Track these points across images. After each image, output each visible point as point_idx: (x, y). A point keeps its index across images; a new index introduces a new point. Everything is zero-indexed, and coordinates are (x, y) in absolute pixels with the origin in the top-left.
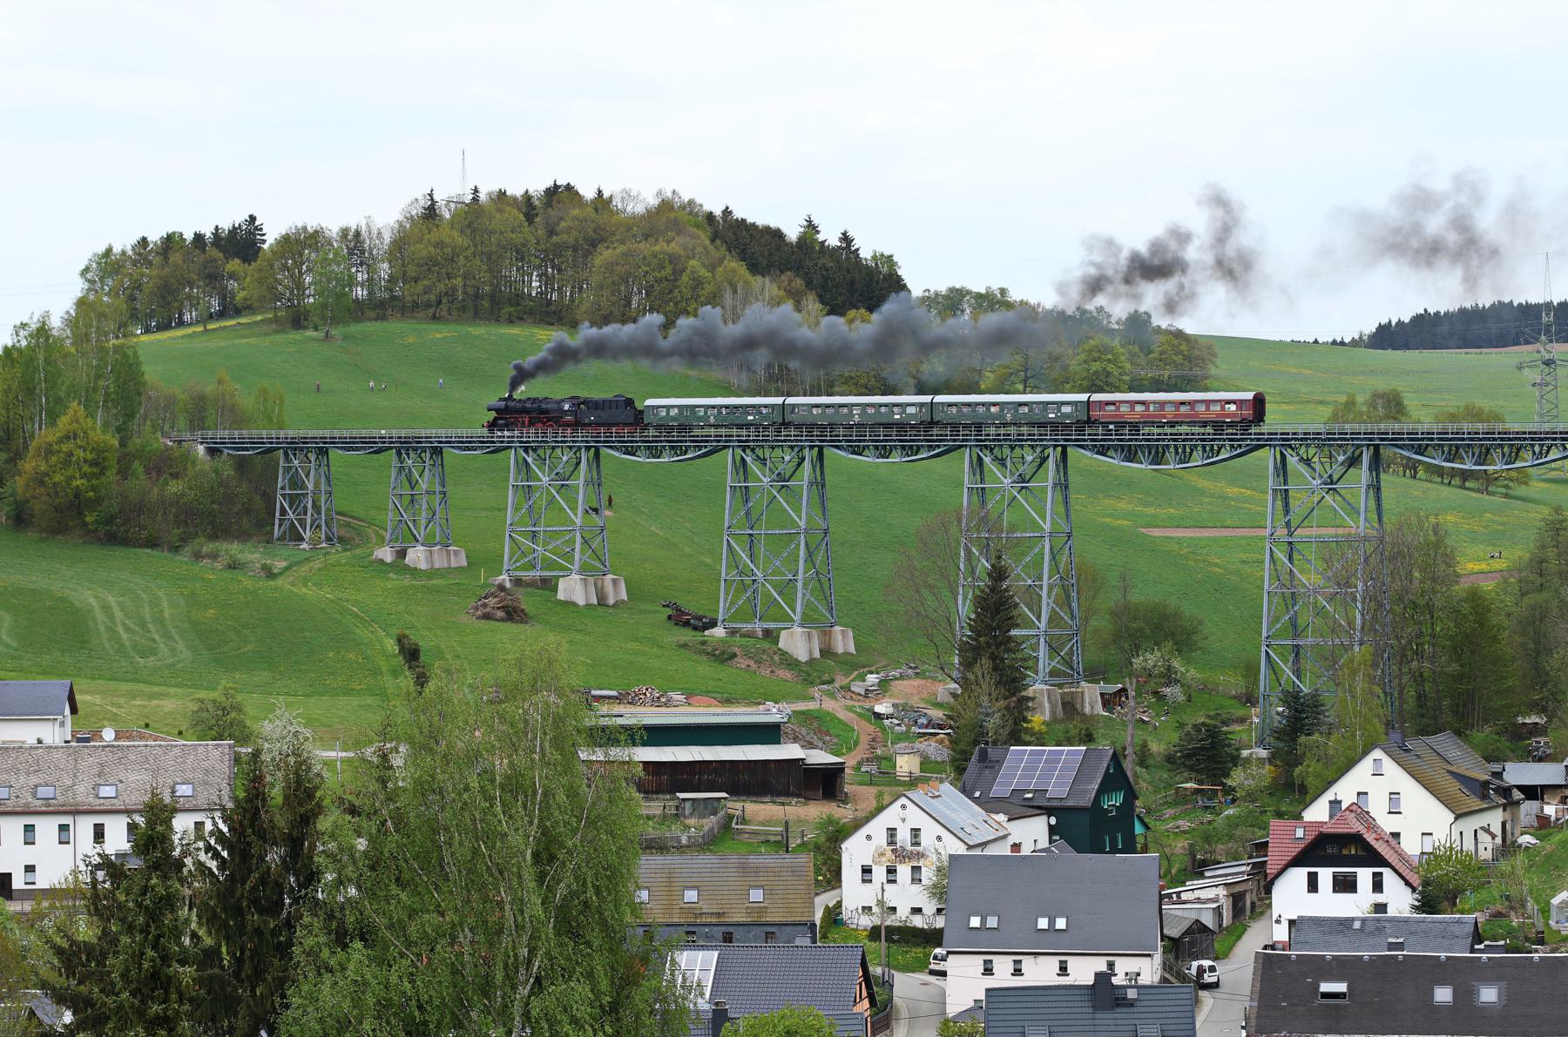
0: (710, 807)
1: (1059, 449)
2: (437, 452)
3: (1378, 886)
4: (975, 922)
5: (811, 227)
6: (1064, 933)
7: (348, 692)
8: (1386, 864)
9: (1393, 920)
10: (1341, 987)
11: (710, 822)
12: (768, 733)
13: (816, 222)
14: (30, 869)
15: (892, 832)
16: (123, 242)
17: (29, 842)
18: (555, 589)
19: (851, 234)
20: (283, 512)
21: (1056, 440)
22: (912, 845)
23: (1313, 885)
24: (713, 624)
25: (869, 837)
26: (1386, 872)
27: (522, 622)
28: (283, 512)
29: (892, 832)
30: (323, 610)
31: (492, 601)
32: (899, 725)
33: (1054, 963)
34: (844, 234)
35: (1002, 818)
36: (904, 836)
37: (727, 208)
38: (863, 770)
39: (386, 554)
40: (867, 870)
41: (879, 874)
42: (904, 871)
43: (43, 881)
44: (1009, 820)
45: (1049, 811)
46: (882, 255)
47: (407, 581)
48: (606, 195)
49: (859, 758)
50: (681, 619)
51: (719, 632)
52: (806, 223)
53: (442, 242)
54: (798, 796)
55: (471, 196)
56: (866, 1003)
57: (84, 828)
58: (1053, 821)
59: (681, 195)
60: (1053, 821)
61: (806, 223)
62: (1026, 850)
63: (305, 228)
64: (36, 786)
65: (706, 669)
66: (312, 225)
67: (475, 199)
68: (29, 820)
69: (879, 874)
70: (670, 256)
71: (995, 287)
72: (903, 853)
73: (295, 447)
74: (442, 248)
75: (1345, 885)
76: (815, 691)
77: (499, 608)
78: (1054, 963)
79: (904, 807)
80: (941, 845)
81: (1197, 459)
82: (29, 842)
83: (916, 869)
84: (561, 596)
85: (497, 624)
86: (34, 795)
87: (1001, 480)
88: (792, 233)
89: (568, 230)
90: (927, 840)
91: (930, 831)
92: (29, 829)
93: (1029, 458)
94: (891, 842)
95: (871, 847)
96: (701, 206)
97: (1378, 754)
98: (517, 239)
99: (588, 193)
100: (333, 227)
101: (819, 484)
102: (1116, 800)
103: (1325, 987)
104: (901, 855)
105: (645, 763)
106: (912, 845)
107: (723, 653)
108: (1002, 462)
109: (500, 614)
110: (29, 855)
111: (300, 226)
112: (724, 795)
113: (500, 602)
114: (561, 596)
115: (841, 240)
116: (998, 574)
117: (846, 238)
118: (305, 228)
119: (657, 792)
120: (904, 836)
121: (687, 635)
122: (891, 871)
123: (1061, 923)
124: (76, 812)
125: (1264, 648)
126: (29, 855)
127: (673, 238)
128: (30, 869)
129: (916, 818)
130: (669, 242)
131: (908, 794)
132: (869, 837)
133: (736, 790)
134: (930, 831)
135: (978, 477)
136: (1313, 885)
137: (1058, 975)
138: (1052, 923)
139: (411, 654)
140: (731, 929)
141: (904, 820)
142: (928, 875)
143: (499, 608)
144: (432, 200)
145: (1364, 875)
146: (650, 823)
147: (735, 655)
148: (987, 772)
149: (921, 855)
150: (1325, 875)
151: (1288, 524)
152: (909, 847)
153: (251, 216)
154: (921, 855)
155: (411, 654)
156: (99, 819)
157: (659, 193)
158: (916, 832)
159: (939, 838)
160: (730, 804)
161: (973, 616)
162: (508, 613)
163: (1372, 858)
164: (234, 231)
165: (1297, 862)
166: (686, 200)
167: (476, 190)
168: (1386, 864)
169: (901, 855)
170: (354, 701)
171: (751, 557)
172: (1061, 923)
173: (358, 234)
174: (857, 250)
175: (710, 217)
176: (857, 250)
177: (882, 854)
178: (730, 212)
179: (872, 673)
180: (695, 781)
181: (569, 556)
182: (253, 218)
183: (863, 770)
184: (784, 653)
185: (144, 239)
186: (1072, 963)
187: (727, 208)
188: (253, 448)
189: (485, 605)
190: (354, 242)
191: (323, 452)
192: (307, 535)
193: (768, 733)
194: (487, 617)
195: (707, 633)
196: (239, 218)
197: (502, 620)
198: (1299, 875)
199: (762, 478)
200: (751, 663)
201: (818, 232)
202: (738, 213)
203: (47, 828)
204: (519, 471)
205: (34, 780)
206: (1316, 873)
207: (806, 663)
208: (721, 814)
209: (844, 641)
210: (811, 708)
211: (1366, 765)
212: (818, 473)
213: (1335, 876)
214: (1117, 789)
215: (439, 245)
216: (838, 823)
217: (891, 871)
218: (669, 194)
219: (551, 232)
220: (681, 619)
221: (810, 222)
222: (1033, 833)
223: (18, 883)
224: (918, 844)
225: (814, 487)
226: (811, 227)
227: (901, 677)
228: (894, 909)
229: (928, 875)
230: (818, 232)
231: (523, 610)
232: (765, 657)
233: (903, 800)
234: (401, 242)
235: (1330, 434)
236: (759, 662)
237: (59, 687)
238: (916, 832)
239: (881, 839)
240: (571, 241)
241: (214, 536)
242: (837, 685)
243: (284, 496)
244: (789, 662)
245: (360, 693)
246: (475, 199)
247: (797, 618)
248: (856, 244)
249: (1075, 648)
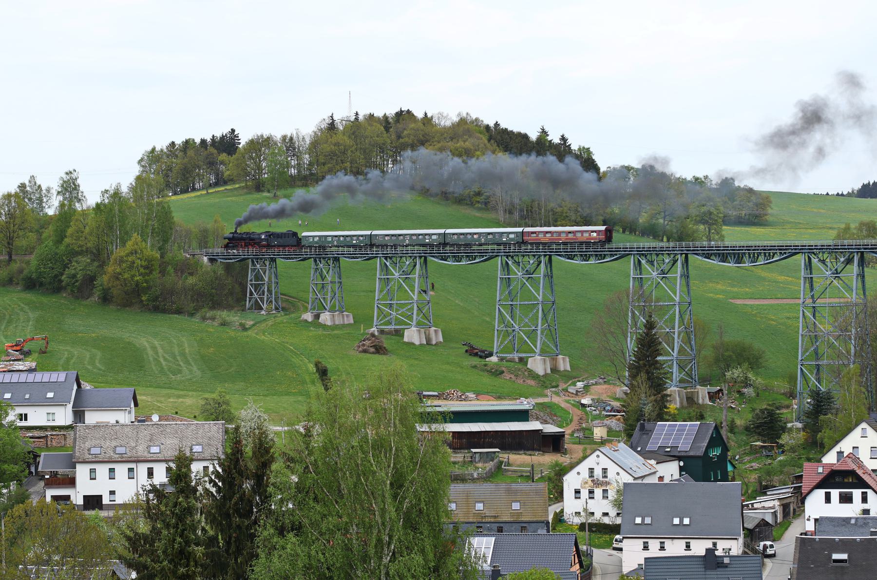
0: (490, 457)
1: (684, 255)
2: (337, 259)
3: (864, 499)
4: (638, 520)
5: (544, 132)
6: (688, 527)
7: (288, 394)
8: (869, 487)
9: (873, 518)
10: (844, 556)
11: (490, 465)
12: (522, 415)
13: (546, 129)
14: (112, 493)
15: (591, 470)
16: (162, 144)
18: (402, 336)
19: (566, 136)
20: (251, 294)
21: (682, 251)
22: (603, 477)
23: (828, 499)
24: (491, 354)
25: (578, 473)
26: (869, 491)
27: (384, 354)
28: (251, 294)
29: (591, 470)
30: (274, 348)
31: (367, 343)
32: (595, 410)
33: (682, 543)
34: (562, 136)
35: (653, 462)
36: (598, 473)
37: (497, 122)
38: (575, 435)
39: (308, 317)
40: (577, 492)
41: (585, 494)
42: (598, 492)
43: (119, 499)
44: (657, 463)
45: (679, 458)
46: (584, 148)
47: (320, 332)
48: (429, 115)
49: (573, 429)
50: (472, 352)
51: (494, 359)
52: (541, 130)
53: (338, 143)
54: (539, 450)
55: (354, 117)
56: (578, 566)
57: (142, 469)
58: (682, 464)
59: (471, 115)
60: (682, 464)
61: (541, 130)
62: (667, 480)
63: (262, 136)
64: (115, 447)
65: (487, 380)
66: (266, 134)
67: (357, 119)
68: (112, 466)
69: (585, 494)
70: (465, 149)
72: (598, 482)
74: (338, 146)
75: (846, 499)
76: (548, 392)
77: (371, 346)
78: (682, 543)
79: (598, 456)
80: (619, 477)
81: (761, 261)
82: (112, 478)
83: (605, 491)
84: (406, 339)
85: (370, 355)
86: (114, 452)
87: (651, 273)
88: (534, 136)
89: (409, 135)
90: (611, 475)
91: (613, 470)
92: (112, 470)
93: (667, 261)
96: (482, 121)
97: (864, 425)
98: (380, 140)
99: (419, 115)
100: (278, 135)
101: (549, 276)
102: (716, 452)
103: (835, 556)
104: (597, 483)
105: (454, 433)
106: (603, 477)
107: (496, 371)
108: (651, 263)
109: (372, 350)
110: (112, 485)
111: (259, 135)
112: (497, 450)
113: (372, 343)
114: (406, 339)
115: (561, 139)
116: (650, 326)
117: (563, 139)
118: (262, 136)
119: (460, 449)
120: (598, 473)
121: (476, 361)
122: (591, 492)
123: (686, 521)
124: (137, 461)
125: (799, 366)
126: (112, 485)
127: (467, 139)
128: (112, 493)
129: (605, 462)
130: (465, 141)
132: (578, 473)
133: (504, 447)
134: (613, 470)
135: (638, 271)
136: (828, 499)
137: (685, 550)
138: (681, 521)
139: (323, 373)
140: (502, 525)
141: (598, 464)
142: (612, 494)
143: (371, 346)
144: (333, 119)
145: (857, 493)
146: (457, 466)
147: (503, 372)
148: (645, 436)
149: (608, 483)
150: (835, 493)
151: (813, 297)
152: (601, 479)
153: (232, 130)
154: (608, 483)
155: (323, 373)
156: (150, 465)
157: (459, 114)
158: (605, 470)
159: (618, 474)
160: (501, 455)
161: (636, 349)
162: (376, 349)
163: (862, 484)
164: (223, 138)
165: (819, 486)
166: (474, 118)
167: (357, 114)
168: (868, 487)
169: (597, 483)
170: (292, 399)
171: (512, 317)
172: (686, 521)
173: (291, 139)
174: (570, 145)
175: (487, 127)
176: (570, 145)
178: (499, 125)
179: (579, 381)
180: (481, 443)
181: (410, 317)
182: (233, 131)
183: (575, 435)
184: (530, 371)
185: (173, 143)
186: (693, 543)
187: (497, 122)
188: (235, 259)
189: (364, 345)
190: (289, 143)
192: (265, 306)
193: (522, 415)
194: (365, 351)
195: (487, 359)
196: (226, 130)
197: (373, 353)
198: (820, 493)
199: (518, 273)
200: (512, 376)
201: (548, 135)
202: (503, 126)
203: (121, 470)
204: (382, 270)
205: (114, 444)
206: (830, 493)
207: (543, 376)
208: (495, 461)
209: (564, 364)
210: (546, 401)
211: (857, 432)
212: (549, 270)
213: (840, 494)
214: (717, 446)
215: (337, 144)
216: (561, 466)
217: (591, 492)
218: (465, 115)
219: (399, 137)
220: (472, 352)
221: (543, 129)
222: (670, 470)
223: (106, 501)
224: (606, 477)
225: (547, 278)
226: (544, 132)
227: (596, 384)
228: (593, 514)
229: (612, 494)
230: (548, 135)
231: (385, 348)
232: (520, 373)
233: (598, 453)
234: (316, 143)
235: (836, 246)
236: (517, 376)
237: (128, 392)
238: (605, 470)
239: (585, 474)
240: (410, 141)
241: (213, 308)
242: (560, 388)
243: (251, 285)
244: (533, 375)
245: (294, 394)
246: (357, 119)
247: (537, 351)
248: (569, 142)
249: (693, 367)
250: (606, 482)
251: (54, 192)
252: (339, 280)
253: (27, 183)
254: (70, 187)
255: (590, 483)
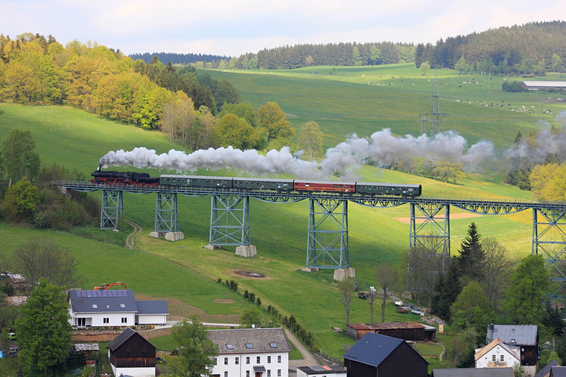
15: (494, 356)
17: (226, 363)
29: (494, 356)
36: (498, 357)
54: (423, 340)
58: (523, 350)
64: (226, 345)
79: (498, 348)
84: (237, 253)
86: (227, 347)
92: (226, 359)
94: (494, 360)
95: (487, 361)
114: (237, 253)
120: (498, 357)
124: (241, 354)
141: (498, 353)
158: (502, 357)
177: (491, 364)
203: (232, 359)
238: (502, 357)
239: (491, 359)
250: (503, 363)
255: (493, 364)
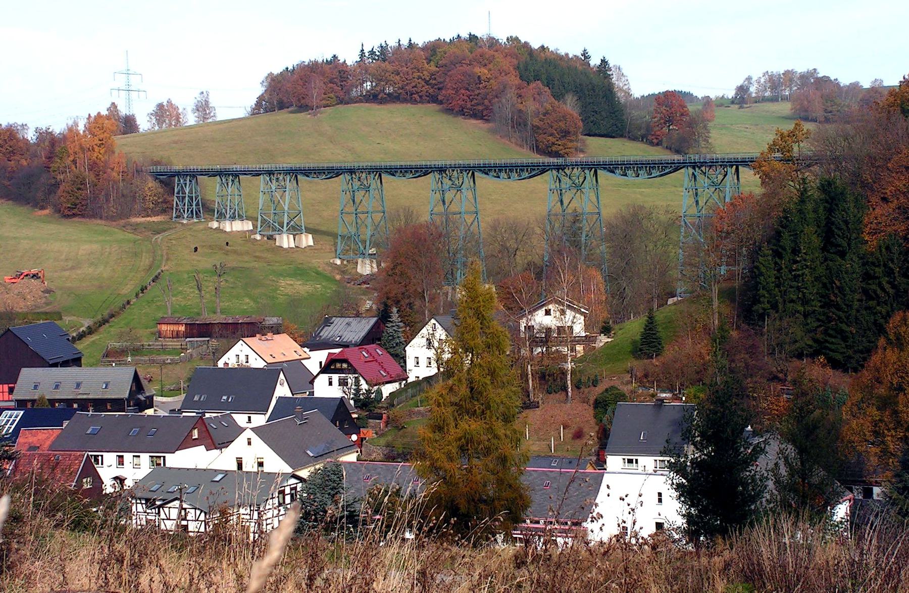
4: (196, 398)
5: (585, 54)
23: (330, 384)
35: (306, 349)
36: (243, 359)
44: (310, 351)
62: (230, 366)
71: (811, 68)
73: (178, 174)
120: (243, 359)
131: (243, 339)
134: (252, 356)
150: (335, 377)
152: (244, 364)
188: (166, 175)
191: (194, 176)
198: (324, 377)
224: (247, 362)
225: (470, 190)
226: (585, 54)
251: (189, 109)
252: (239, 194)
253: (165, 104)
254: (203, 108)
